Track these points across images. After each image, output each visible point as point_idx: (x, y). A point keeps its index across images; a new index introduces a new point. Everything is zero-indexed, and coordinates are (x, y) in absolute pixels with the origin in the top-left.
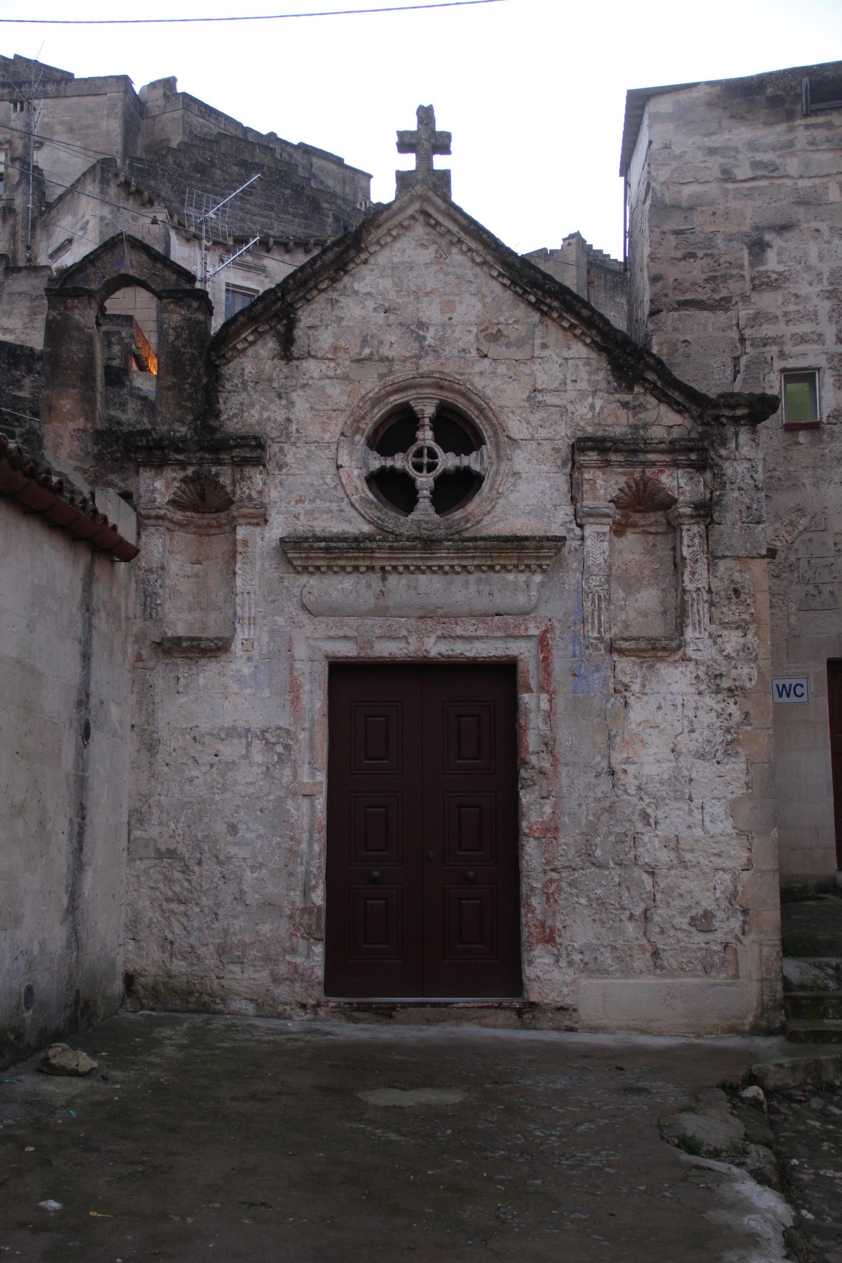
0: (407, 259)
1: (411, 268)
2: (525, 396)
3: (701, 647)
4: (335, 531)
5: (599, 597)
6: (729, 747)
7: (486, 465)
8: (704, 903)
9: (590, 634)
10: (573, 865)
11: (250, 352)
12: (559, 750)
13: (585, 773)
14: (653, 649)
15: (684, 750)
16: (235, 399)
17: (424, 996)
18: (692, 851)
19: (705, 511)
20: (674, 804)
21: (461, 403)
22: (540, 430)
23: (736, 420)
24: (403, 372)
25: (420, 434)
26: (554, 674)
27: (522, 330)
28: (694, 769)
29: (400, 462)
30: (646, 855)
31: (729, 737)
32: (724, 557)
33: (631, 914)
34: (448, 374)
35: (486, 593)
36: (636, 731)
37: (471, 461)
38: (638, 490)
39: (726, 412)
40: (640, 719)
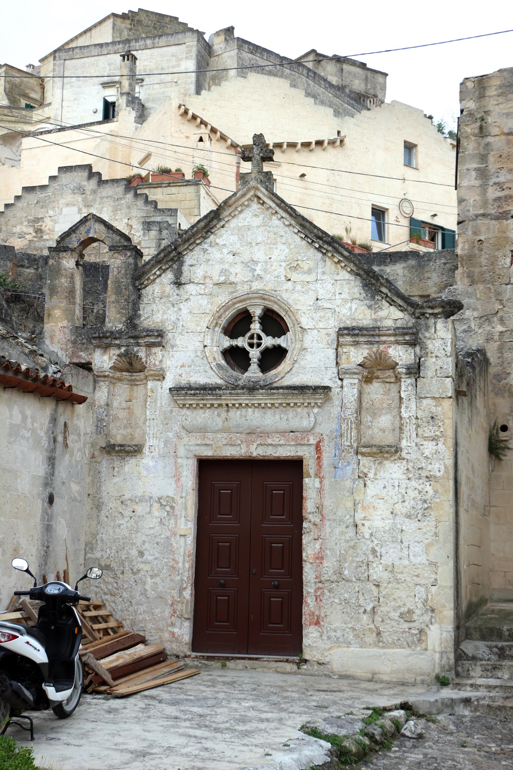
0: (247, 224)
1: (249, 229)
2: (311, 303)
3: (410, 451)
4: (202, 383)
5: (351, 421)
6: (425, 511)
7: (289, 343)
8: (408, 605)
9: (345, 443)
10: (331, 579)
11: (157, 281)
12: (325, 512)
13: (340, 525)
14: (381, 452)
15: (399, 513)
16: (148, 309)
17: (248, 654)
18: (402, 573)
19: (415, 370)
20: (392, 545)
21: (275, 308)
22: (320, 323)
23: (435, 315)
24: (242, 290)
25: (252, 326)
26: (323, 467)
27: (311, 264)
28: (404, 525)
29: (241, 342)
30: (375, 575)
31: (426, 506)
32: (426, 398)
33: (365, 609)
34: (267, 292)
35: (284, 419)
36: (371, 501)
37: (281, 341)
38: (376, 358)
39: (430, 311)
40: (373, 494)
